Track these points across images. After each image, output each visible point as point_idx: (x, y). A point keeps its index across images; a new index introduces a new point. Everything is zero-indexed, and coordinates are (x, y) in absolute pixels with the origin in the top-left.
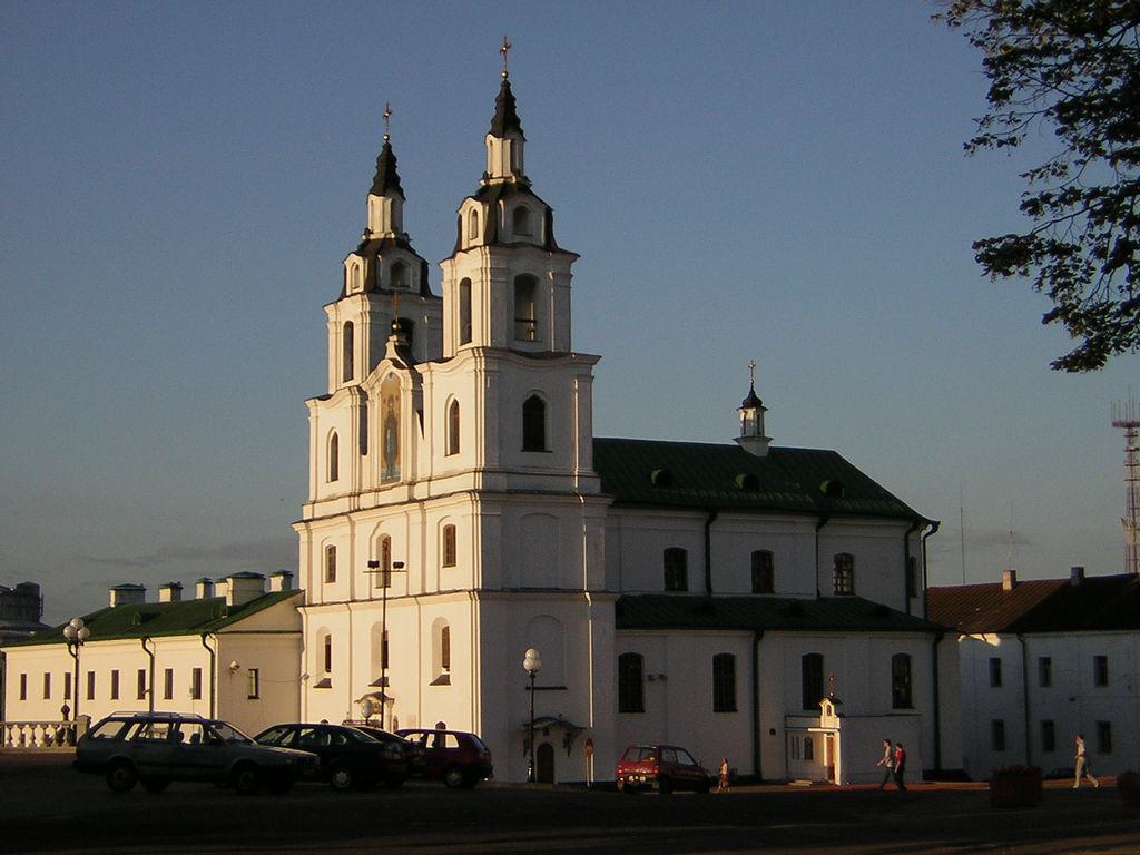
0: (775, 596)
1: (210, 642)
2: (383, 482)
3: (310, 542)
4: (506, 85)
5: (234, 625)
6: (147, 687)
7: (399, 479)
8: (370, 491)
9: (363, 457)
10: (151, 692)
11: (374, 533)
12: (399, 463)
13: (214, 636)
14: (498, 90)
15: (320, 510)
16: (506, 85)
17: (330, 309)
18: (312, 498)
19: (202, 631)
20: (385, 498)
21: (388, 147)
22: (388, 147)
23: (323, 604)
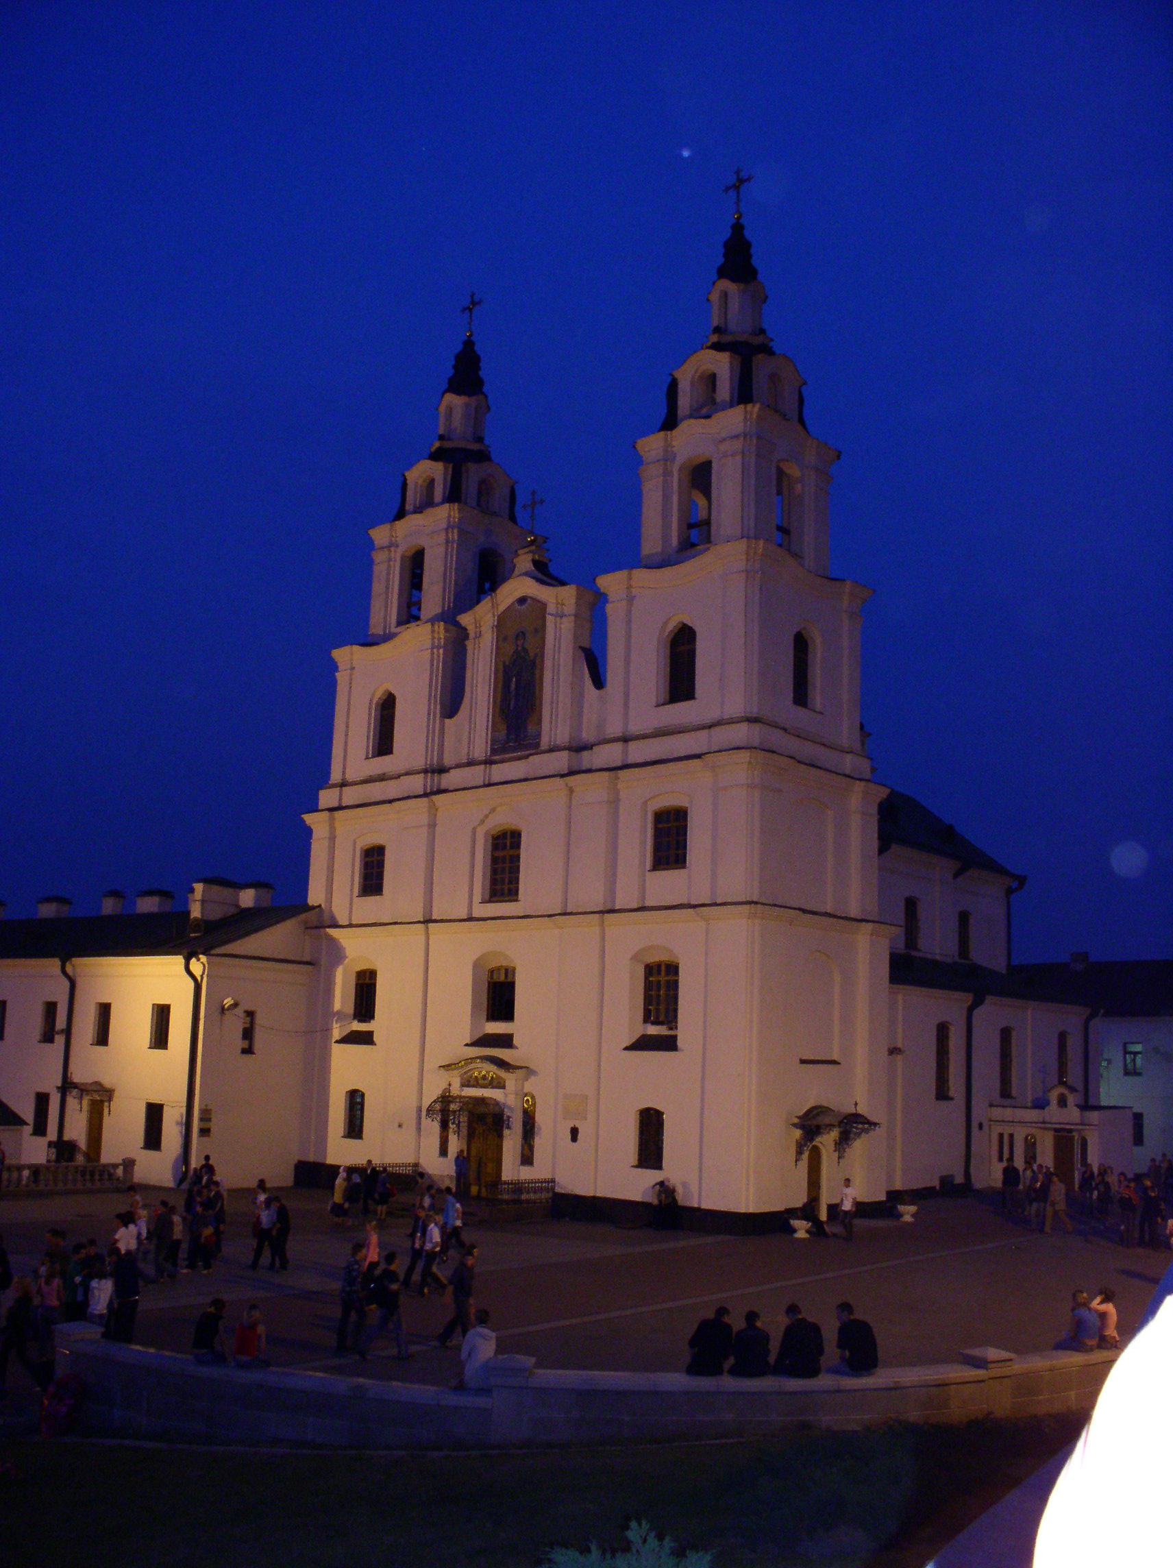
0: (921, 954)
1: (196, 967)
3: (332, 838)
5: (223, 948)
6: (61, 1023)
7: (538, 745)
8: (459, 766)
9: (447, 721)
10: (68, 1032)
11: (482, 822)
13: (203, 958)
14: (727, 234)
15: (351, 795)
17: (380, 535)
18: (335, 776)
19: (185, 952)
20: (500, 771)
22: (469, 344)
23: (351, 926)
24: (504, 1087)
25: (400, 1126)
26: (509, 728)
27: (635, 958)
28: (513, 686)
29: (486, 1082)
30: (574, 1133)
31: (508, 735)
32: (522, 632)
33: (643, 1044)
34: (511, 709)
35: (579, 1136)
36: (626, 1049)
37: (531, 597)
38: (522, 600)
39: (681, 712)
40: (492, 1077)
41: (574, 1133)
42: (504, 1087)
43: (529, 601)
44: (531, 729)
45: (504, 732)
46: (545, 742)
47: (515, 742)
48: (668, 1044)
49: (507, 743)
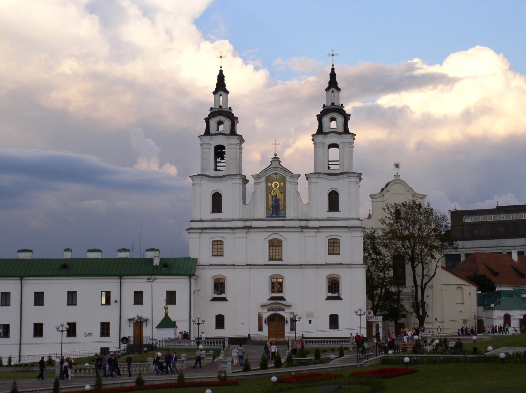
2: (267, 217)
4: (333, 69)
7: (285, 217)
12: (285, 210)
16: (333, 69)
21: (221, 71)
22: (221, 71)
24: (284, 311)
25: (242, 324)
26: (273, 210)
27: (326, 277)
28: (274, 198)
29: (277, 310)
30: (310, 322)
31: (273, 213)
32: (276, 184)
33: (329, 298)
34: (274, 205)
35: (312, 322)
36: (326, 299)
38: (276, 174)
39: (334, 214)
40: (279, 308)
41: (310, 322)
42: (284, 311)
43: (278, 174)
44: (282, 212)
45: (272, 212)
46: (288, 216)
48: (339, 298)
49: (272, 215)
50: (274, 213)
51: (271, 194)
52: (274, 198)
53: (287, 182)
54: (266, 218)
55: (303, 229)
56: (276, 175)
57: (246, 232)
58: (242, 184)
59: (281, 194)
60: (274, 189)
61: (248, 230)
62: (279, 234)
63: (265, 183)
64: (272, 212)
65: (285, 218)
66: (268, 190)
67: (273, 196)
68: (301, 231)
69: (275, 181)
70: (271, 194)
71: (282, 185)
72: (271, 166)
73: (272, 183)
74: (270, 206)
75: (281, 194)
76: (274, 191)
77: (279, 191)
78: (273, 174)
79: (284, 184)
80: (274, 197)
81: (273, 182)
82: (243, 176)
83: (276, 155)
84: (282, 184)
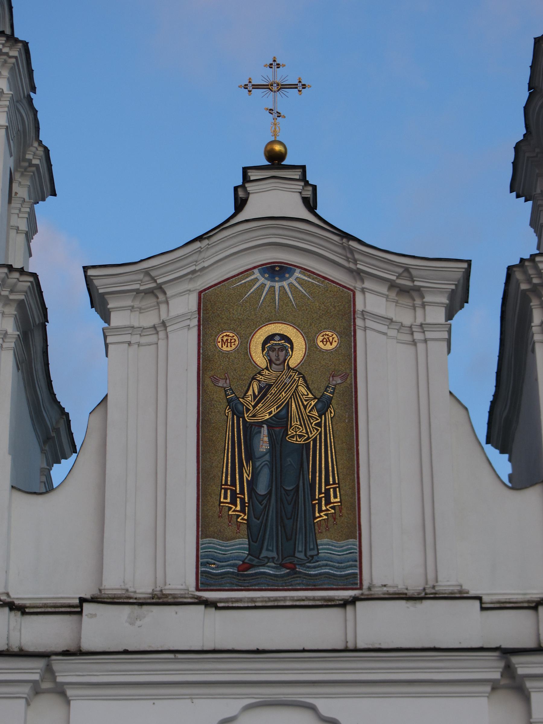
32: (284, 337)
34: (262, 489)
37: (304, 270)
43: (297, 274)
47: (283, 566)
49: (252, 566)
50: (264, 554)
51: (238, 413)
52: (266, 439)
53: (369, 323)
54: (198, 589)
55: (515, 660)
56: (283, 278)
57: (26, 690)
58: (11, 344)
59: (322, 413)
60: (268, 376)
61: (40, 663)
62: (312, 708)
63: (194, 332)
64: (251, 537)
65: (361, 588)
66: (215, 380)
67: (260, 425)
68: (497, 676)
69: (269, 321)
70: (238, 413)
71: (329, 347)
72: (241, 217)
73: (252, 334)
74: (234, 493)
75: (322, 413)
76: (265, 390)
77: (302, 390)
78: (257, 274)
79: (340, 335)
80: (265, 430)
81: (258, 326)
82: (25, 283)
83: (282, 156)
84: (325, 341)
